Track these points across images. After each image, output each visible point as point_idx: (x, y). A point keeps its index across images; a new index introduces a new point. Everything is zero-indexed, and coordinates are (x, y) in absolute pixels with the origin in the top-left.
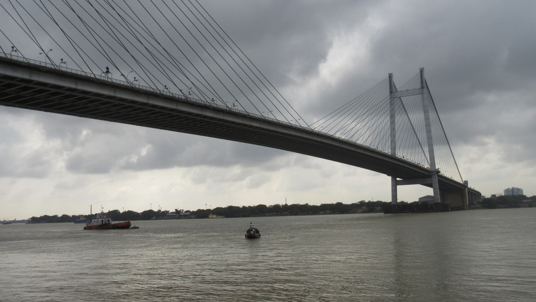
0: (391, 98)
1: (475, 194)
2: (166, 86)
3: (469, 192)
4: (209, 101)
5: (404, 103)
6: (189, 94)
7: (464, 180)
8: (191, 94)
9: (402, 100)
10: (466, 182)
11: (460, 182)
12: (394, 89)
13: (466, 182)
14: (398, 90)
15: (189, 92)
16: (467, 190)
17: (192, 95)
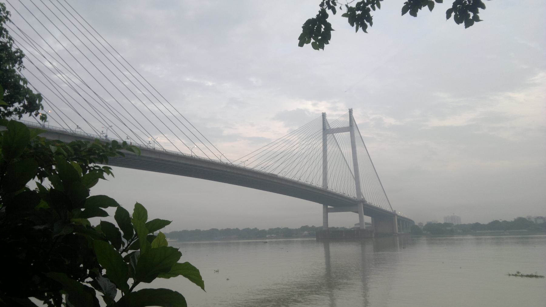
0: (323, 134)
1: (405, 222)
2: (102, 131)
3: (398, 220)
4: (146, 144)
5: (336, 139)
6: (127, 139)
7: (394, 209)
8: (129, 139)
9: (335, 136)
10: (395, 211)
11: (390, 211)
12: (327, 125)
13: (395, 211)
14: (331, 127)
15: (127, 137)
16: (396, 217)
17: (130, 139)
